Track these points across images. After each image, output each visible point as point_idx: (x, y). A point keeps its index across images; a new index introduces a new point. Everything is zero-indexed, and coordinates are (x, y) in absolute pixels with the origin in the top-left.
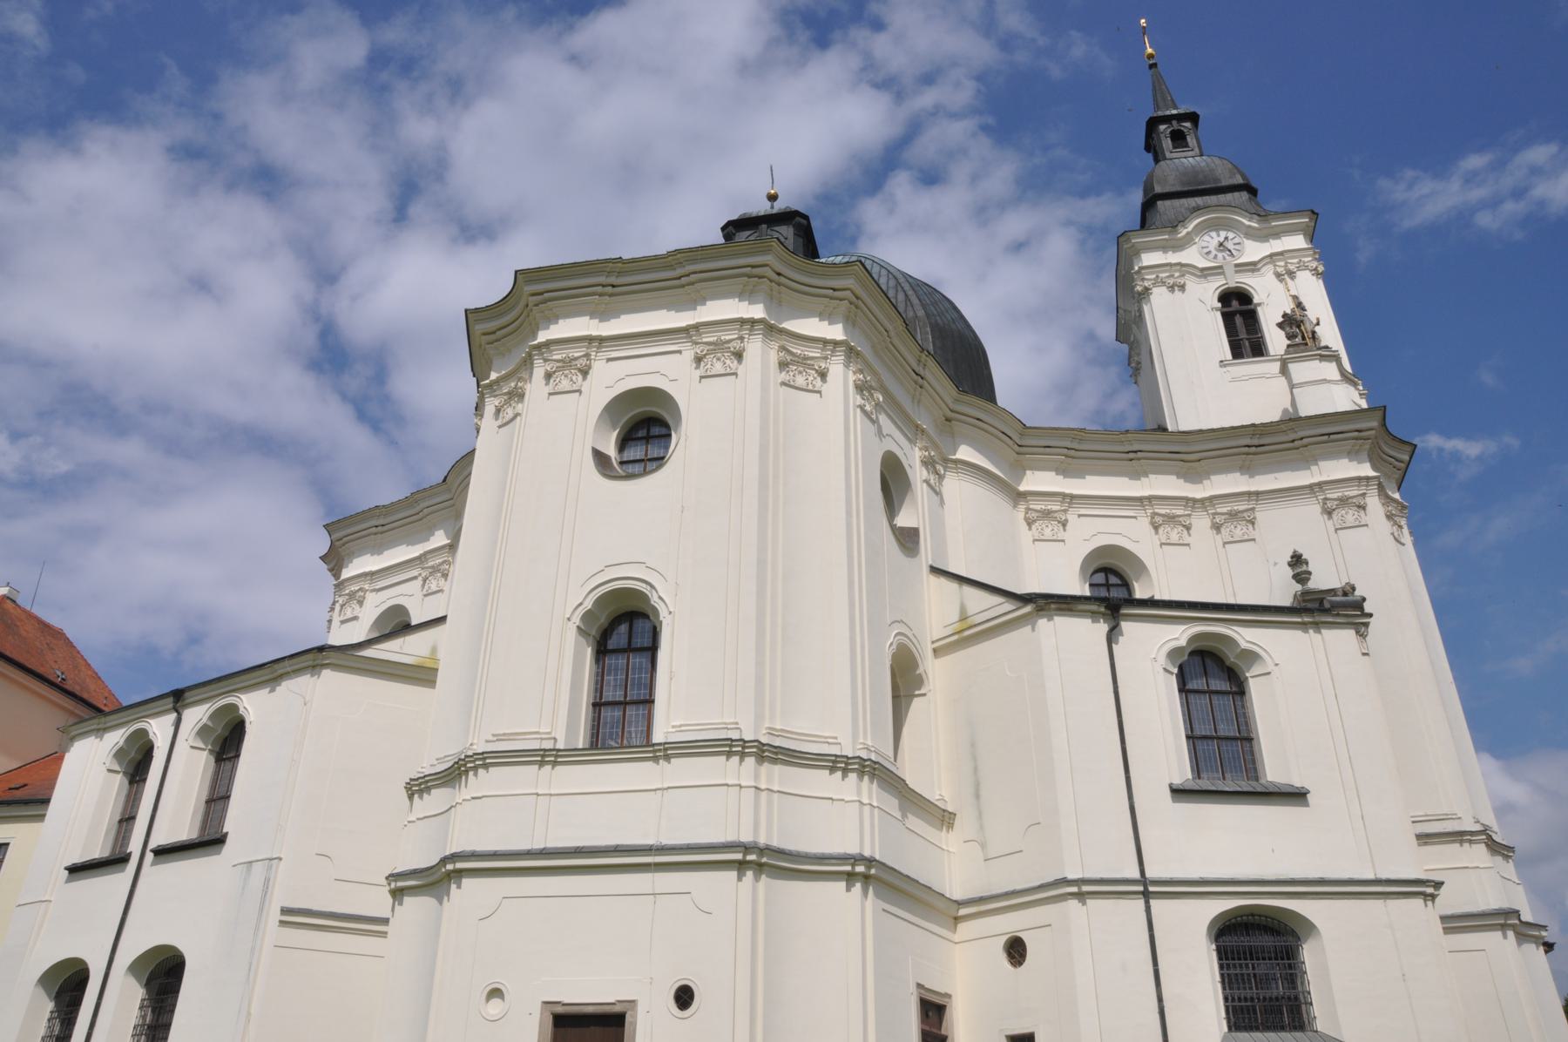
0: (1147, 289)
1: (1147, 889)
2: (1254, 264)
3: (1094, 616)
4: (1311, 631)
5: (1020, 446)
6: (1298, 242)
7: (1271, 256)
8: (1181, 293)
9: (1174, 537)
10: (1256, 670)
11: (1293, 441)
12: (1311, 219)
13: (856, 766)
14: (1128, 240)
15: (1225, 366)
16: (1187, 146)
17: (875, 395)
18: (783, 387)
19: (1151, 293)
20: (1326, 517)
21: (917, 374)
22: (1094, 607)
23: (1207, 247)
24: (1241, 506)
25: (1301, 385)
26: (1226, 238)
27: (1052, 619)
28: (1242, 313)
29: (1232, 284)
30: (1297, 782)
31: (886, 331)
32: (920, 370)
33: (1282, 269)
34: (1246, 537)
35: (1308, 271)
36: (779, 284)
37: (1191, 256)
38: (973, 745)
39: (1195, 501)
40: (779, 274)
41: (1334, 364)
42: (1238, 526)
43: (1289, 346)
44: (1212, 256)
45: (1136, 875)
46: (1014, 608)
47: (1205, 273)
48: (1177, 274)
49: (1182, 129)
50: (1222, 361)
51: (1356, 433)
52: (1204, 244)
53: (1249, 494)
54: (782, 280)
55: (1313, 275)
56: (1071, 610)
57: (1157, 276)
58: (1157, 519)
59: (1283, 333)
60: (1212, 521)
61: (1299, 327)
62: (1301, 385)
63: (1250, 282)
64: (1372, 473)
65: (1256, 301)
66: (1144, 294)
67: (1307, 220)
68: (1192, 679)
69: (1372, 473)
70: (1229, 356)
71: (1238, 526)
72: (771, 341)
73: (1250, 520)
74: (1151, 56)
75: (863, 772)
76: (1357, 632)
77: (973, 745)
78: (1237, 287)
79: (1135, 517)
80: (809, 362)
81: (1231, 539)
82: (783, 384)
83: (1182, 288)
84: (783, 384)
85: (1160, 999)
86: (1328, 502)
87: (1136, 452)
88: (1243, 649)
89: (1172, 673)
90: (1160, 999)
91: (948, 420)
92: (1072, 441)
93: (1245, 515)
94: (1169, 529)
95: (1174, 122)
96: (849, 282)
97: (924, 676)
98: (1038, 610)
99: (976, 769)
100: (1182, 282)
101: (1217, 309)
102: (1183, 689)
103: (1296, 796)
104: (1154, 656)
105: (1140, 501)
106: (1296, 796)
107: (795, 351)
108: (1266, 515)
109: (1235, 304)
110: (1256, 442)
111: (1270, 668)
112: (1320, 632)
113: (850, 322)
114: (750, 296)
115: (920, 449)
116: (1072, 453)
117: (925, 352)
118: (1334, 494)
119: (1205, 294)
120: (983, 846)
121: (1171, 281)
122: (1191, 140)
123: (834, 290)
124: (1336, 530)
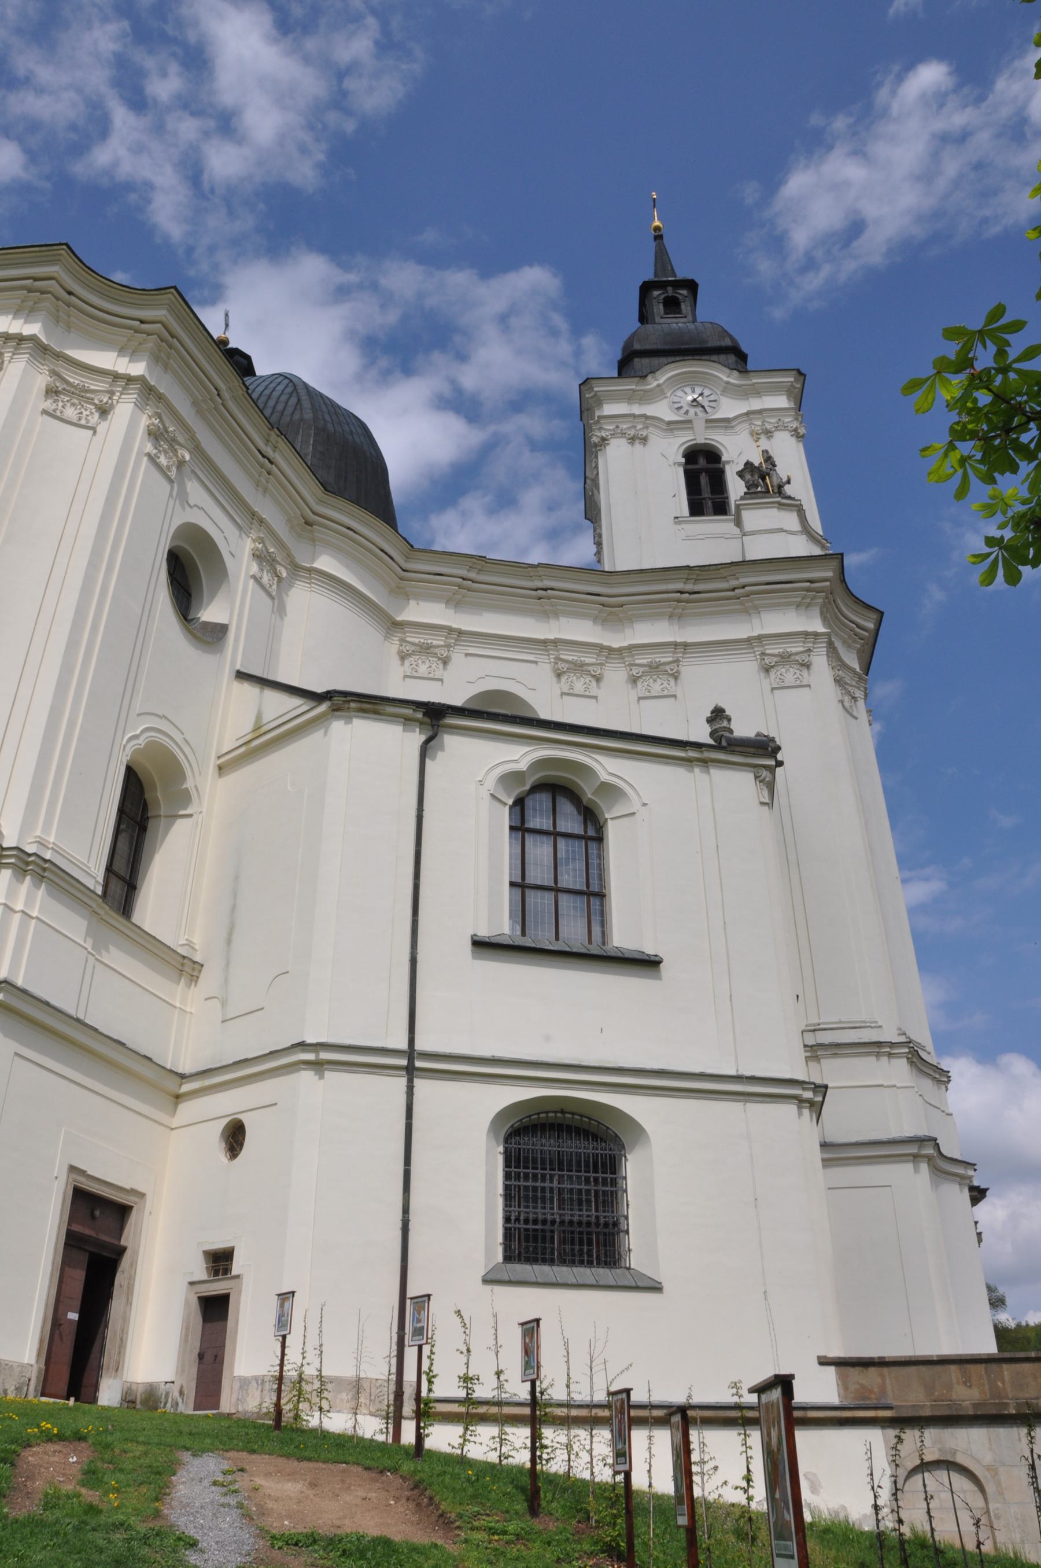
0: (604, 439)
3: (407, 721)
4: (697, 770)
5: (404, 570)
6: (781, 401)
7: (748, 414)
8: (642, 446)
9: (579, 687)
10: (619, 810)
11: (733, 590)
12: (796, 380)
13: (12, 860)
14: (592, 388)
15: (680, 523)
16: (680, 312)
17: (180, 452)
18: (44, 415)
19: (608, 444)
20: (762, 675)
21: (264, 456)
22: (408, 712)
23: (680, 402)
24: (666, 658)
25: (753, 533)
26: (701, 394)
27: (351, 722)
28: (707, 471)
29: (701, 440)
30: (650, 949)
31: (216, 389)
32: (268, 451)
33: (759, 428)
34: (666, 693)
35: (787, 432)
36: (69, 305)
37: (662, 410)
38: (236, 878)
39: (610, 650)
40: (70, 293)
41: (795, 514)
42: (658, 680)
43: (745, 493)
44: (683, 411)
45: (403, 1045)
46: (308, 708)
47: (672, 426)
48: (639, 426)
49: (677, 295)
50: (676, 518)
51: (808, 584)
52: (676, 399)
53: (676, 645)
55: (792, 435)
56: (376, 712)
57: (617, 427)
58: (561, 665)
59: (743, 483)
60: (628, 674)
61: (763, 479)
62: (753, 533)
64: (821, 628)
65: (724, 458)
66: (601, 446)
68: (534, 817)
69: (821, 628)
70: (686, 511)
71: (658, 680)
72: (43, 365)
73: (672, 675)
74: (657, 229)
75: (26, 871)
76: (756, 777)
77: (236, 878)
78: (705, 444)
79: (536, 662)
80: (88, 395)
81: (648, 694)
82: (45, 412)
83: (644, 440)
84: (45, 412)
85: (406, 1210)
86: (766, 658)
87: (545, 590)
88: (602, 782)
89: (505, 804)
90: (406, 1210)
91: (308, 523)
92: (469, 571)
93: (668, 668)
94: (575, 678)
95: (670, 289)
96: (160, 313)
97: (193, 793)
98: (334, 710)
99: (234, 908)
100: (645, 434)
101: (679, 464)
102: (520, 829)
103: (649, 964)
104: (480, 779)
105: (544, 644)
106: (649, 964)
107: (72, 380)
108: (693, 670)
109: (702, 462)
110: (689, 587)
111: (636, 807)
112: (708, 773)
113: (156, 359)
114: (28, 316)
115: (254, 541)
117: (275, 430)
118: (774, 649)
120: (224, 1004)
121: (632, 432)
122: (685, 307)
123: (142, 322)
124: (773, 689)
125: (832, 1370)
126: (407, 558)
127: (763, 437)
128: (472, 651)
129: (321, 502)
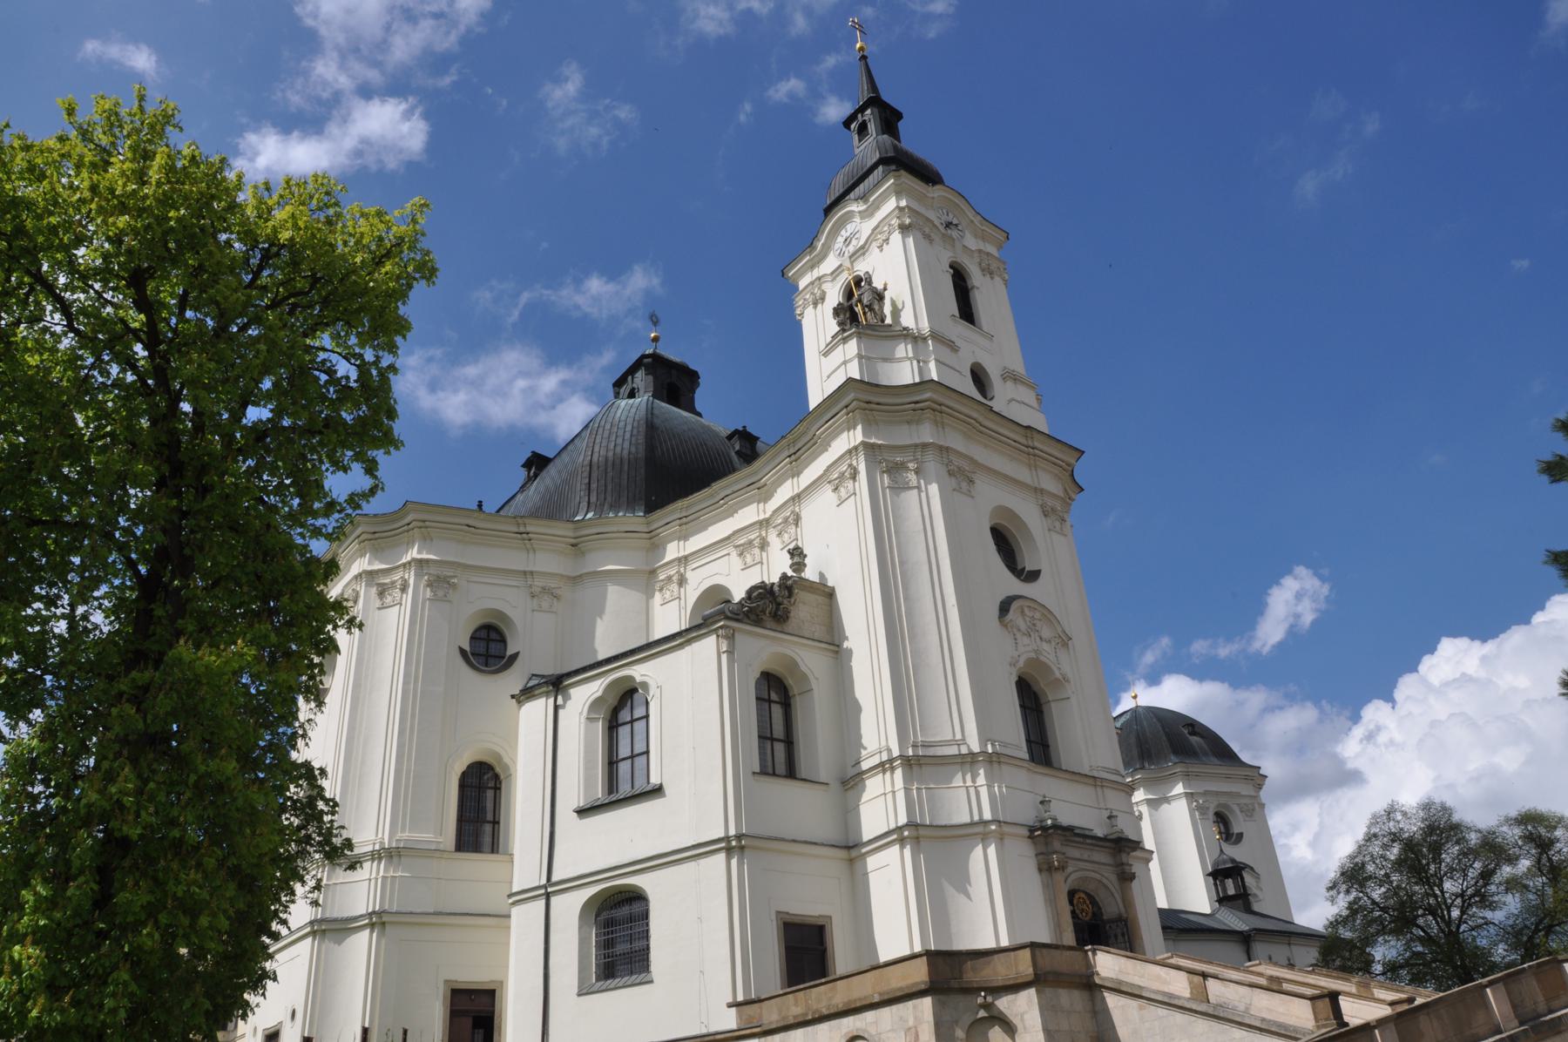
21: (521, 533)
22: (544, 689)
32: (522, 529)
54: (377, 535)
56: (534, 696)
67: (892, 181)
79: (728, 554)
91: (572, 545)
110: (792, 451)
116: (684, 520)
125: (734, 1009)
126: (648, 524)
128: (694, 566)
129: (576, 529)
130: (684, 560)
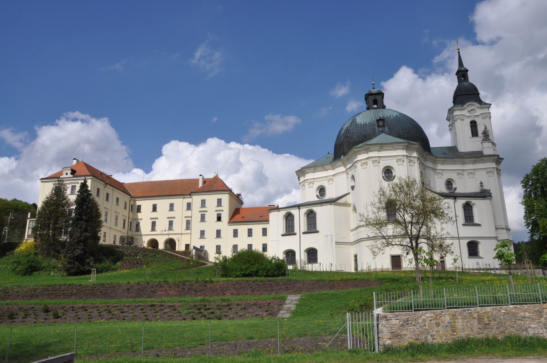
1: (459, 238)
2: (478, 115)
24: (472, 171)
29: (473, 120)
37: (465, 112)
45: (458, 236)
63: (476, 119)
65: (477, 124)
70: (471, 136)
103: (479, 225)
106: (479, 225)
108: (477, 173)
109: (473, 123)
119: (467, 122)
127: (484, 119)
130: (443, 170)
